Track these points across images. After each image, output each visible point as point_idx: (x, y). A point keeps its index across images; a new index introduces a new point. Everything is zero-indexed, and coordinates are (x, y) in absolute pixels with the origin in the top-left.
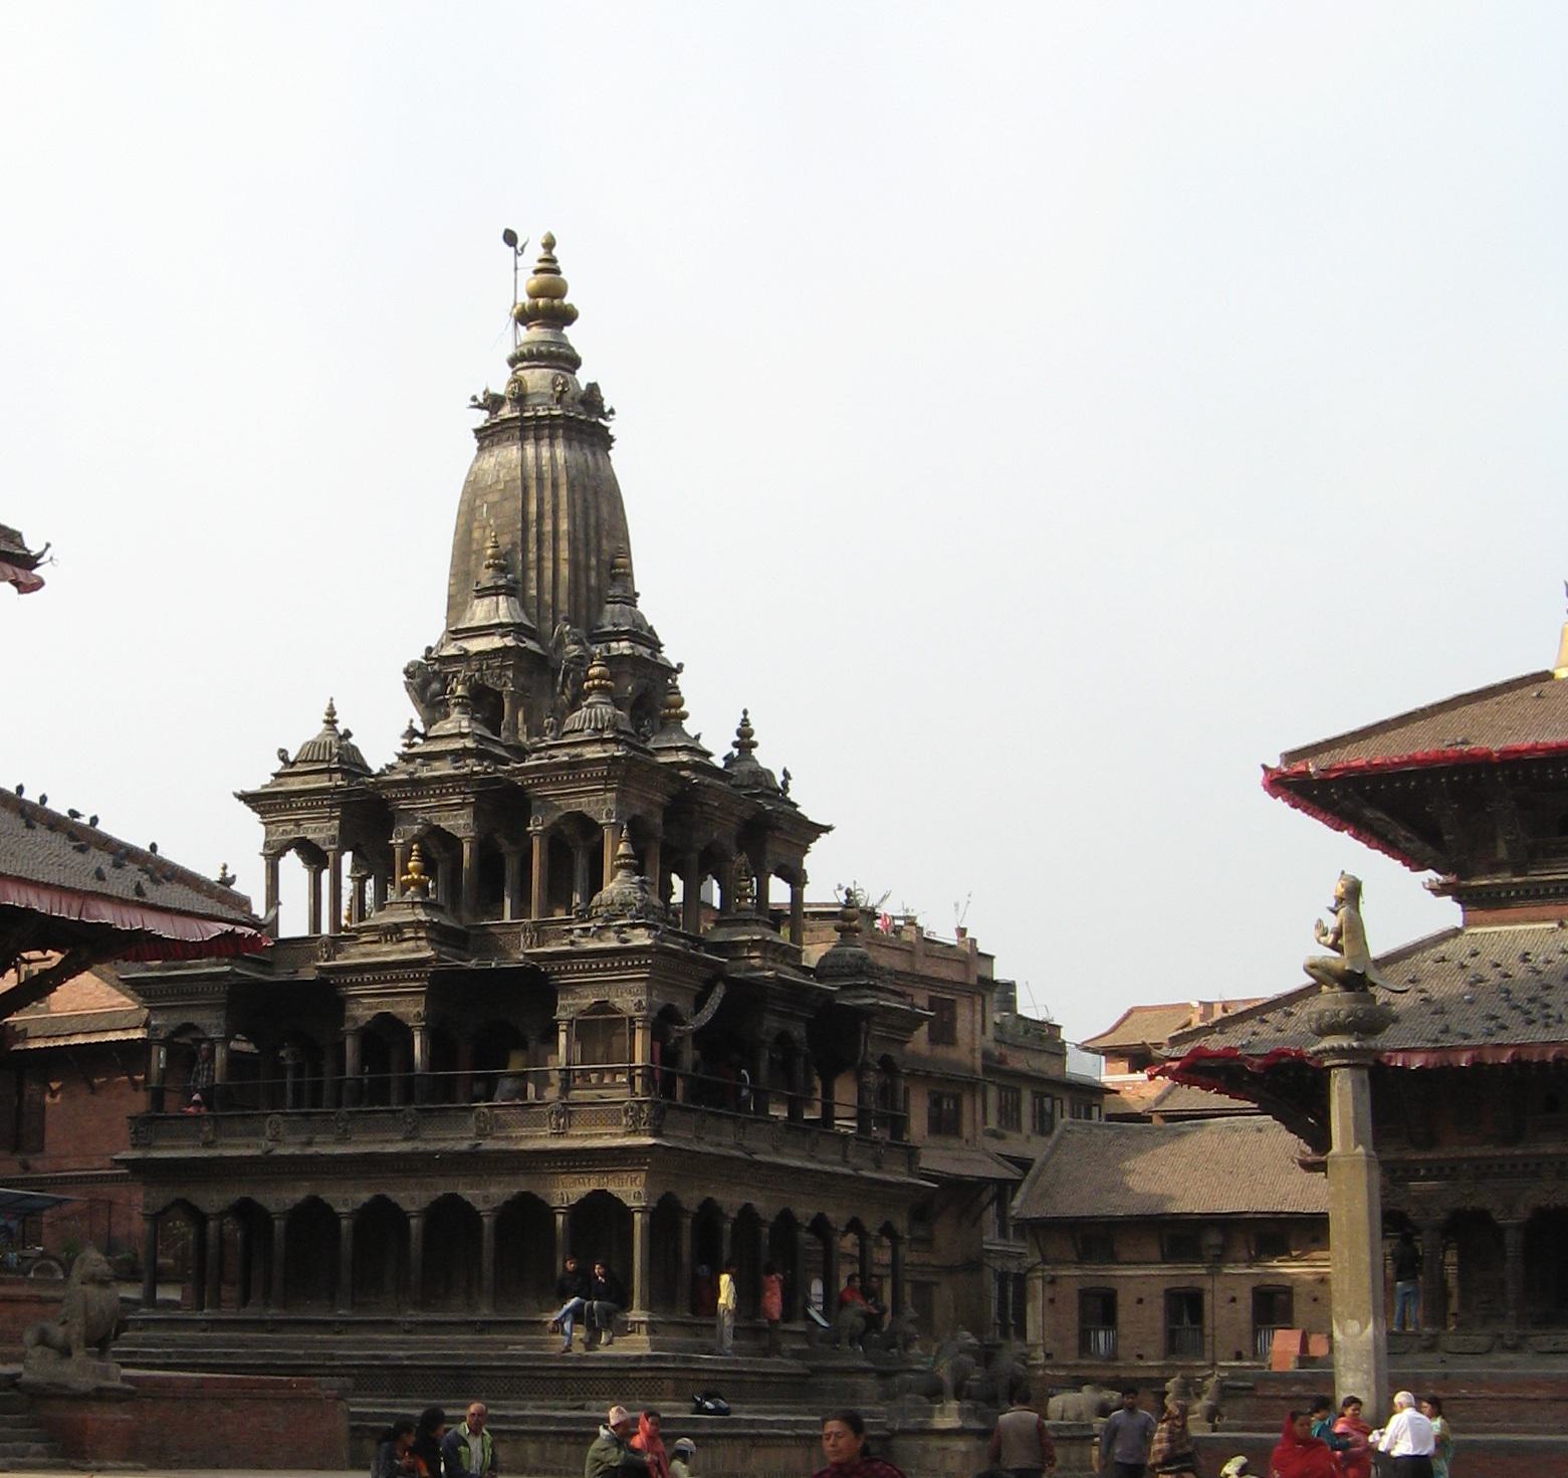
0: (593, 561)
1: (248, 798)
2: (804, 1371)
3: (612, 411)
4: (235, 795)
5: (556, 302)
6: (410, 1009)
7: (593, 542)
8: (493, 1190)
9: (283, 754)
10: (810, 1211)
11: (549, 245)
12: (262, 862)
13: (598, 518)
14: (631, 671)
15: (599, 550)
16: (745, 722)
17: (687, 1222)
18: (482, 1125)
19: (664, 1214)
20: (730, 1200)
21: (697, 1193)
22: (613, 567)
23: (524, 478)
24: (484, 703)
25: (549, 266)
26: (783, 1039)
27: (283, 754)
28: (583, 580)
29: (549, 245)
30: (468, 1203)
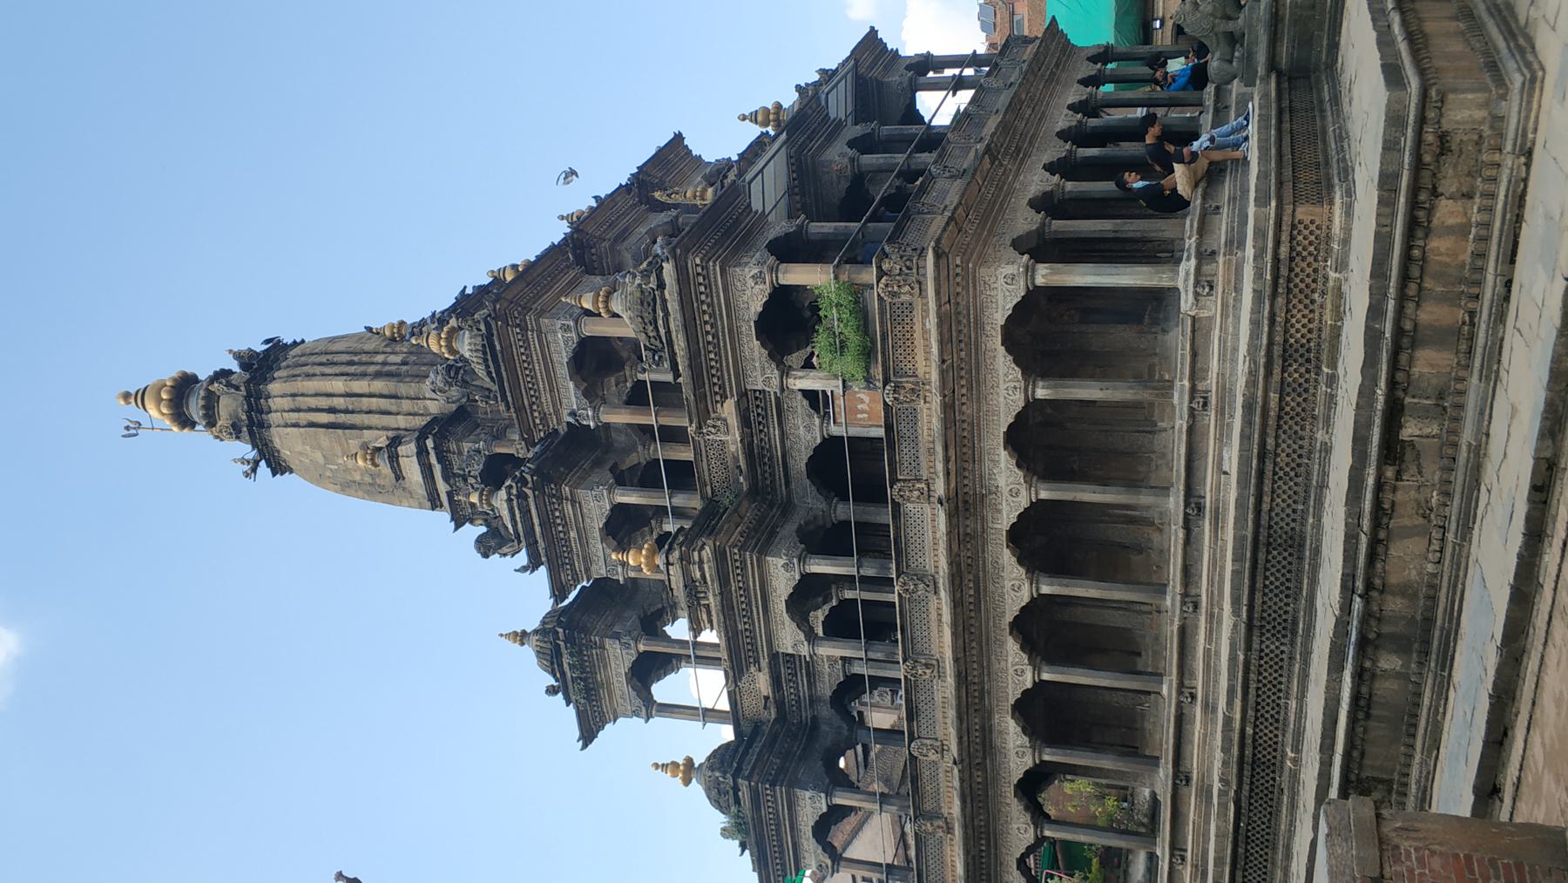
0: (380, 358)
1: (588, 735)
4: (585, 746)
6: (782, 575)
7: (364, 358)
9: (552, 691)
12: (658, 722)
17: (1058, 225)
18: (916, 493)
19: (1040, 248)
20: (1037, 181)
22: (393, 339)
23: (296, 425)
24: (496, 472)
25: (139, 397)
27: (552, 691)
30: (1020, 516)
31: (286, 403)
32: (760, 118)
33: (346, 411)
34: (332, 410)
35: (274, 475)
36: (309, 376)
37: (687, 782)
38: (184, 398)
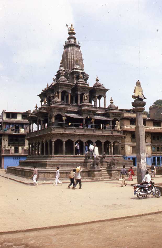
0: (72, 61)
1: (38, 96)
5: (73, 31)
9: (43, 90)
11: (72, 25)
12: (40, 103)
16: (97, 77)
27: (43, 90)
28: (70, 63)
37: (35, 108)
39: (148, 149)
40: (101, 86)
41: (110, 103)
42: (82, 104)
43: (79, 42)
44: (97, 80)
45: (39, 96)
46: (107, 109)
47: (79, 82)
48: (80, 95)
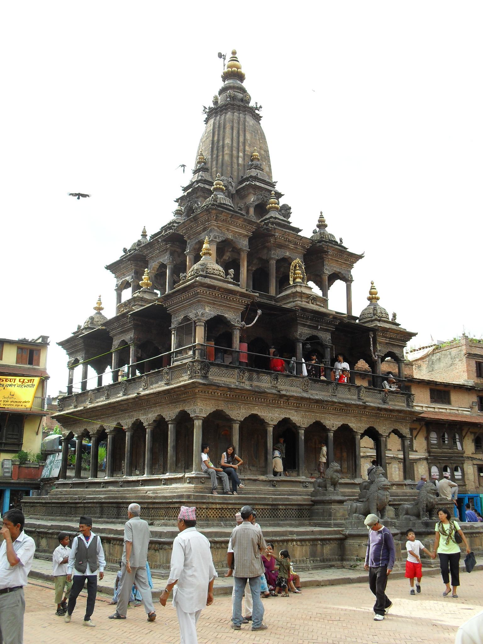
0: (241, 154)
1: (108, 268)
2: (311, 503)
3: (261, 107)
7: (241, 147)
8: (150, 415)
9: (125, 250)
10: (337, 423)
11: (234, 53)
12: (115, 292)
13: (245, 139)
14: (253, 192)
15: (244, 151)
16: (321, 216)
17: (236, 427)
21: (244, 411)
25: (234, 59)
26: (313, 339)
28: (235, 160)
29: (234, 53)
31: (222, 122)
32: (373, 290)
33: (218, 147)
34: (218, 141)
35: (205, 121)
36: (232, 128)
37: (95, 308)
38: (234, 75)
39: (419, 470)
40: (337, 242)
41: (369, 302)
42: (288, 292)
43: (256, 103)
44: (322, 225)
45: (113, 268)
46: (357, 321)
47: (272, 220)
48: (278, 261)
